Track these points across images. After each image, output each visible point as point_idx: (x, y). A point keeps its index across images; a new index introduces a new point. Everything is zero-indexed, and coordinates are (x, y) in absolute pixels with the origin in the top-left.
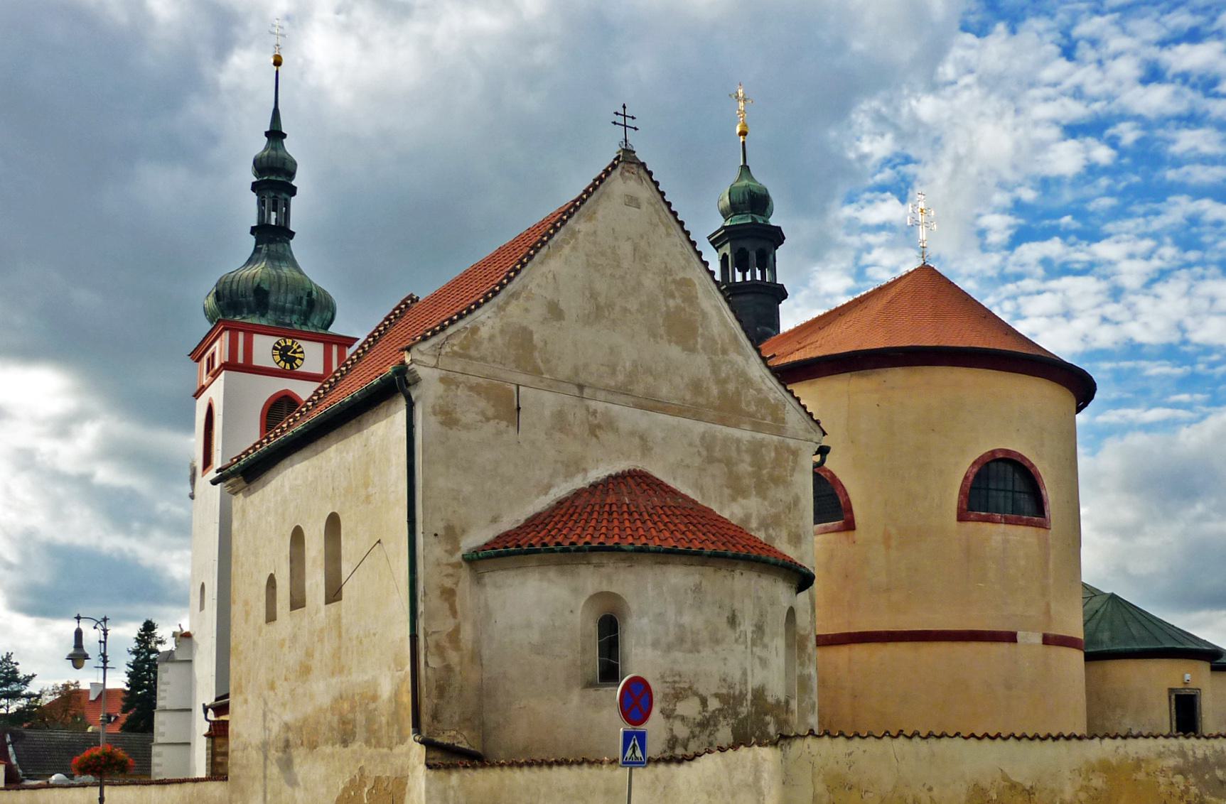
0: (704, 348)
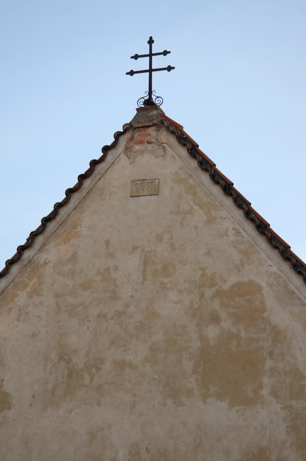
0: (274, 394)
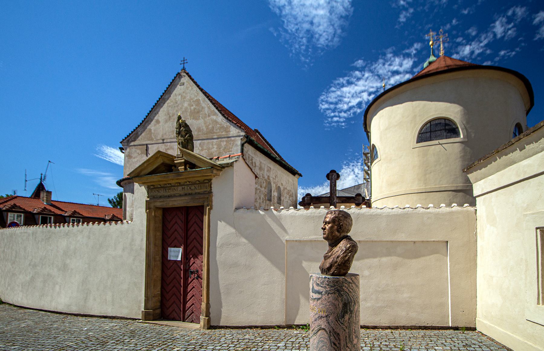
0: (202, 118)
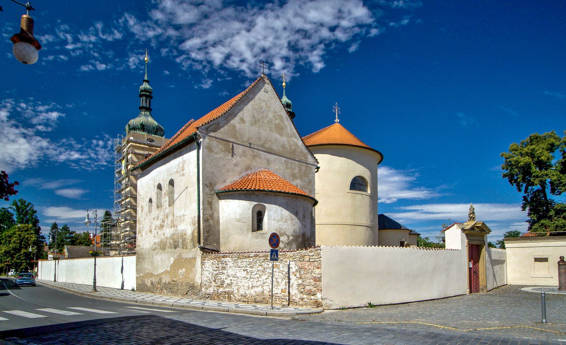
0: (285, 136)
